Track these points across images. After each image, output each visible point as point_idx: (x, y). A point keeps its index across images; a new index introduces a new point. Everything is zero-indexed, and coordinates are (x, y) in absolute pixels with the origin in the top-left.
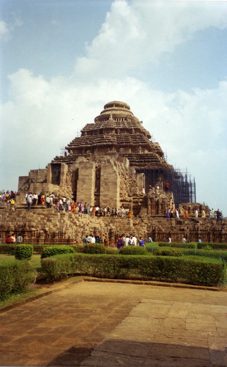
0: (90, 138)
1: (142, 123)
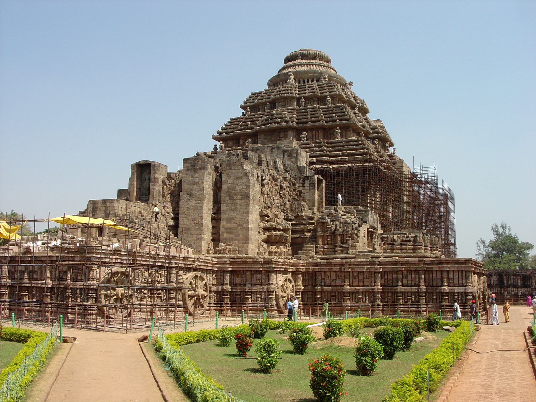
0: (252, 118)
1: (351, 85)
